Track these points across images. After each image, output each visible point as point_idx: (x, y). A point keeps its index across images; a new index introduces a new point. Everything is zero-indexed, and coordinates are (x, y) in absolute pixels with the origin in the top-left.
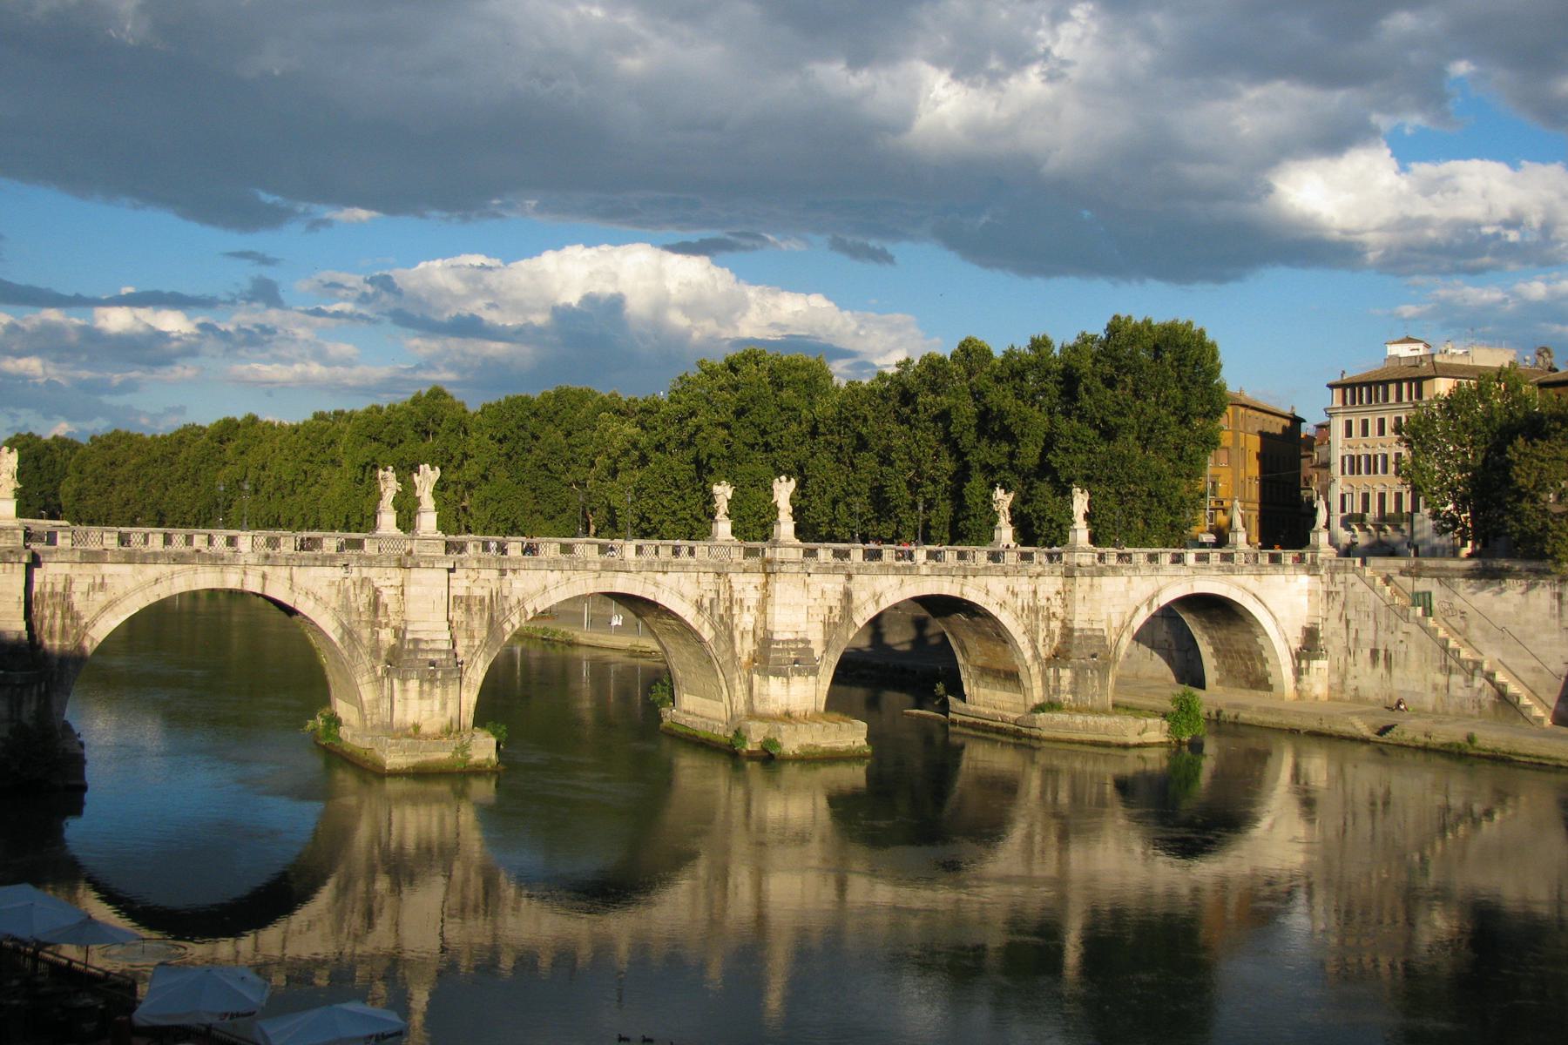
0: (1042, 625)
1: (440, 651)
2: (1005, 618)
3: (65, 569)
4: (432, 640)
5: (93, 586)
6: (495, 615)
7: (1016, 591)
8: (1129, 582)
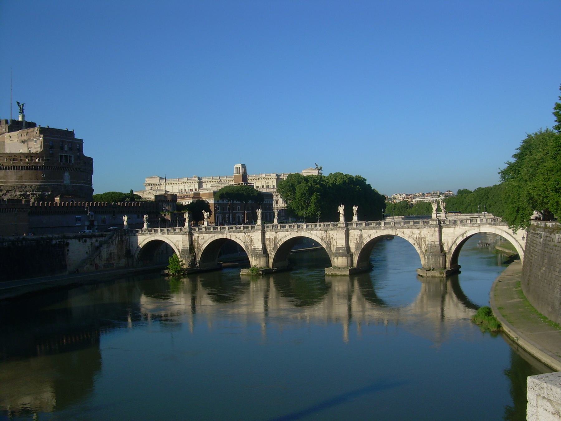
0: (423, 243)
1: (260, 250)
2: (411, 241)
3: (197, 235)
4: (258, 248)
5: (202, 239)
6: (275, 242)
7: (414, 232)
8: (455, 229)
